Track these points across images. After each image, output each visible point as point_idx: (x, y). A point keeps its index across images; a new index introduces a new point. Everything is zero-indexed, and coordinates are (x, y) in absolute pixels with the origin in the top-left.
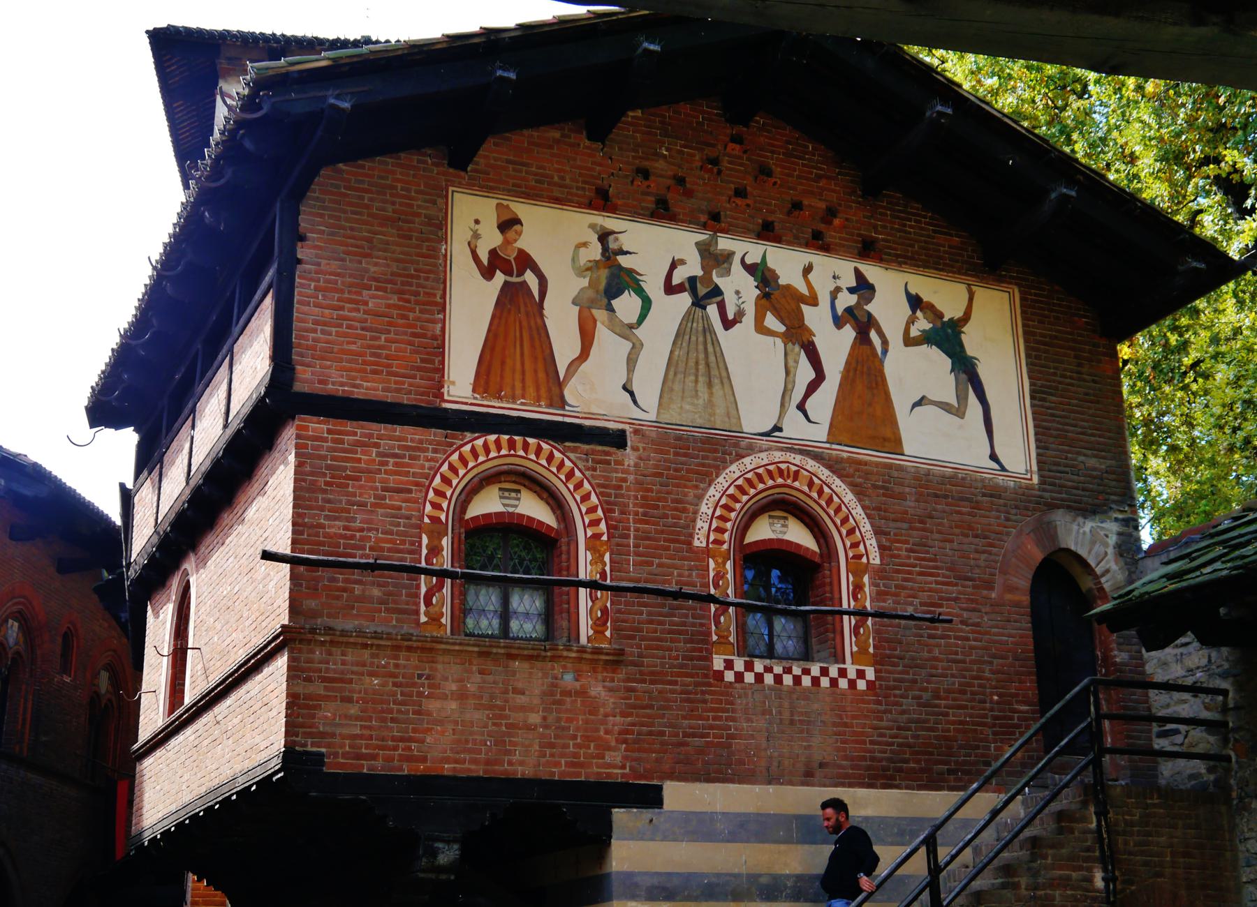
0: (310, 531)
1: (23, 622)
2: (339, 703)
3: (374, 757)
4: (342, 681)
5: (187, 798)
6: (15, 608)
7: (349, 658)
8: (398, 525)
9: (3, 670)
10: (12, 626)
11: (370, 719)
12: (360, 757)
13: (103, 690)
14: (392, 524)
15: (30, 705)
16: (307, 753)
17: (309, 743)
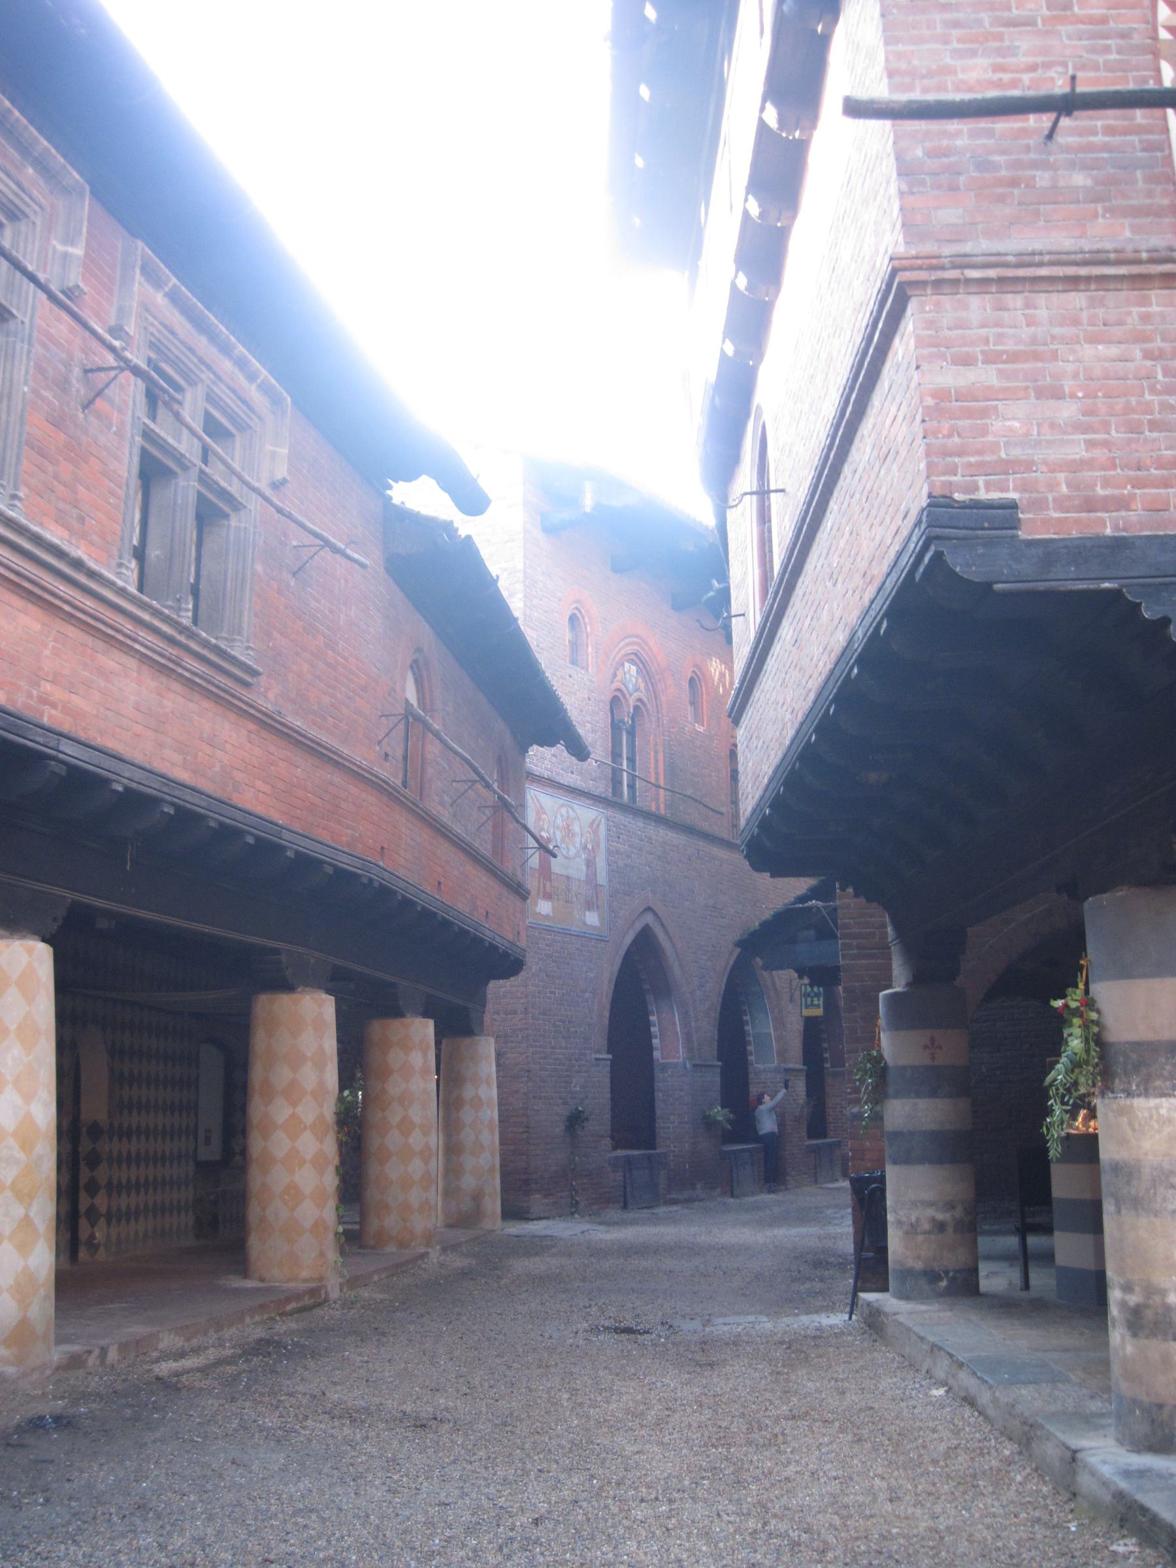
0: (926, 81)
1: (641, 666)
2: (1033, 400)
3: (1122, 504)
4: (1036, 356)
5: (790, 733)
6: (629, 649)
7: (1042, 313)
8: (1107, 50)
9: (626, 719)
10: (629, 670)
11: (1106, 427)
12: (1090, 505)
14: (1093, 50)
15: (661, 756)
16: (977, 505)
17: (981, 484)
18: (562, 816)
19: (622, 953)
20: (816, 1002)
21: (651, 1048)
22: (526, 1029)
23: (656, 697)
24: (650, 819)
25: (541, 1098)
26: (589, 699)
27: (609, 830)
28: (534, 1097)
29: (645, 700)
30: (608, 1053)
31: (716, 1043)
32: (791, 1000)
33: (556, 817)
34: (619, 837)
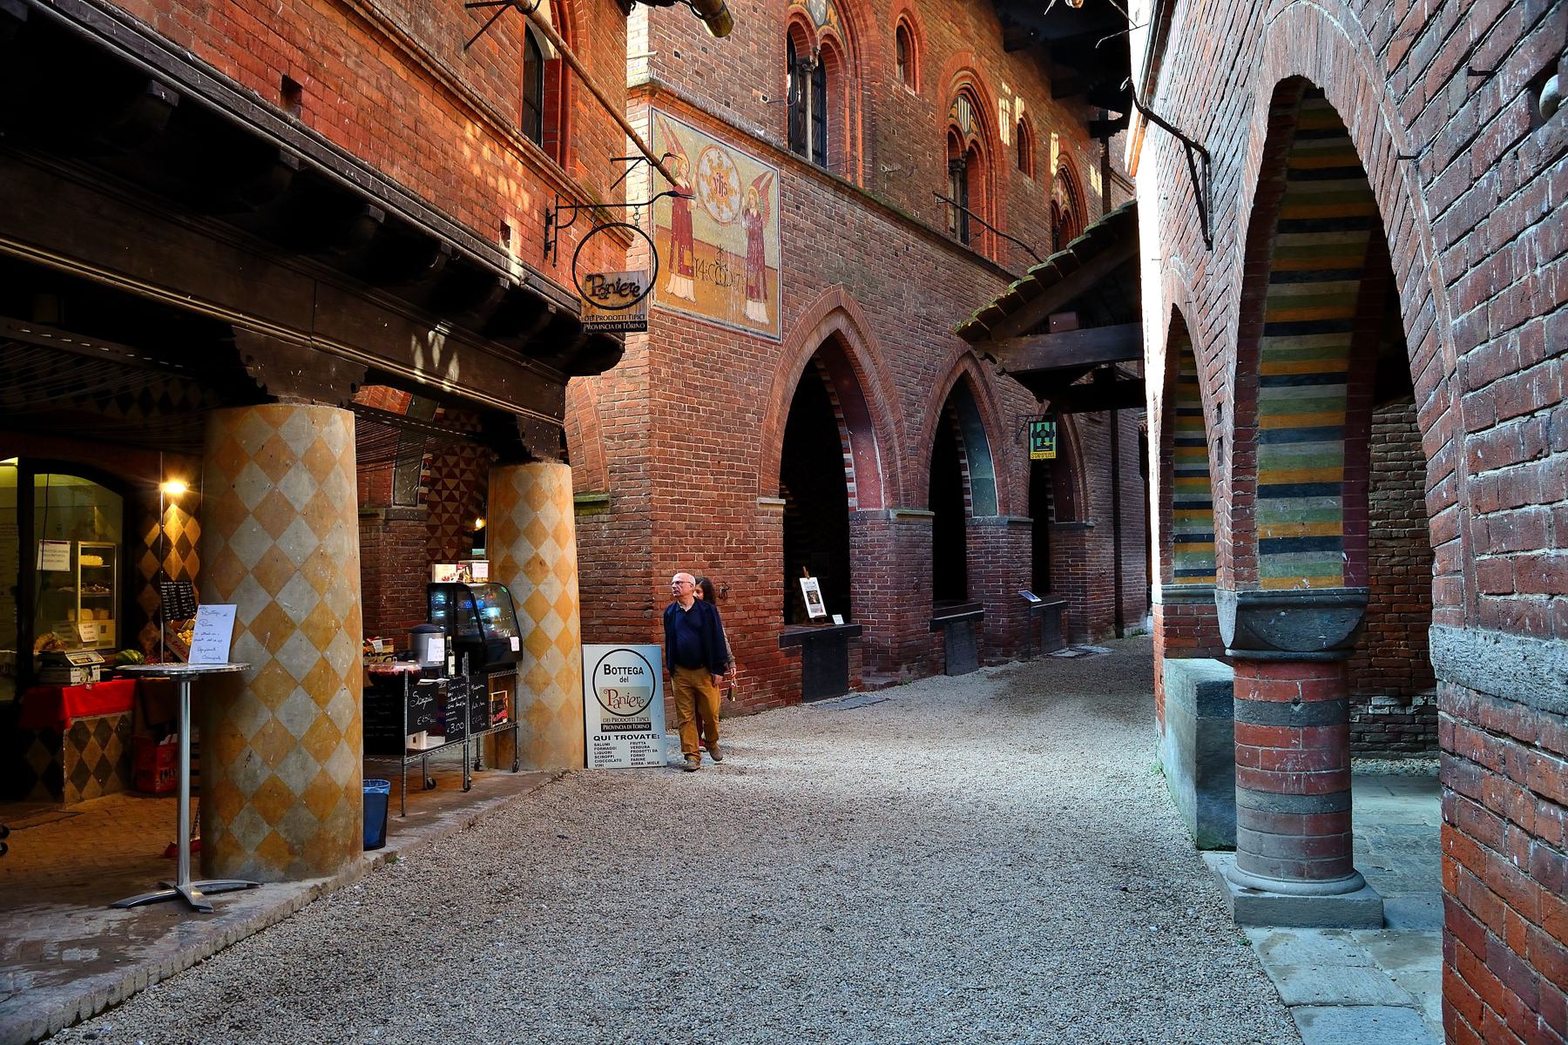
9: (811, 58)
13: (965, 127)
15: (859, 117)
18: (710, 160)
19: (801, 364)
20: (1047, 443)
21: (845, 495)
22: (649, 459)
23: (852, 39)
24: (844, 192)
25: (674, 558)
26: (755, 10)
27: (783, 195)
28: (663, 558)
29: (838, 39)
30: (781, 497)
31: (927, 488)
32: (1018, 441)
33: (700, 160)
34: (798, 208)
